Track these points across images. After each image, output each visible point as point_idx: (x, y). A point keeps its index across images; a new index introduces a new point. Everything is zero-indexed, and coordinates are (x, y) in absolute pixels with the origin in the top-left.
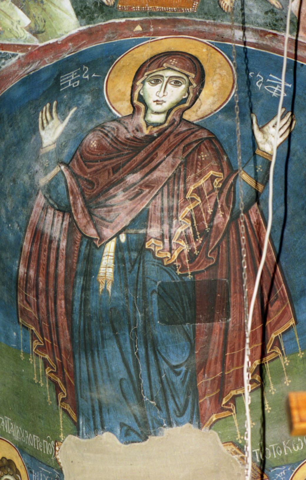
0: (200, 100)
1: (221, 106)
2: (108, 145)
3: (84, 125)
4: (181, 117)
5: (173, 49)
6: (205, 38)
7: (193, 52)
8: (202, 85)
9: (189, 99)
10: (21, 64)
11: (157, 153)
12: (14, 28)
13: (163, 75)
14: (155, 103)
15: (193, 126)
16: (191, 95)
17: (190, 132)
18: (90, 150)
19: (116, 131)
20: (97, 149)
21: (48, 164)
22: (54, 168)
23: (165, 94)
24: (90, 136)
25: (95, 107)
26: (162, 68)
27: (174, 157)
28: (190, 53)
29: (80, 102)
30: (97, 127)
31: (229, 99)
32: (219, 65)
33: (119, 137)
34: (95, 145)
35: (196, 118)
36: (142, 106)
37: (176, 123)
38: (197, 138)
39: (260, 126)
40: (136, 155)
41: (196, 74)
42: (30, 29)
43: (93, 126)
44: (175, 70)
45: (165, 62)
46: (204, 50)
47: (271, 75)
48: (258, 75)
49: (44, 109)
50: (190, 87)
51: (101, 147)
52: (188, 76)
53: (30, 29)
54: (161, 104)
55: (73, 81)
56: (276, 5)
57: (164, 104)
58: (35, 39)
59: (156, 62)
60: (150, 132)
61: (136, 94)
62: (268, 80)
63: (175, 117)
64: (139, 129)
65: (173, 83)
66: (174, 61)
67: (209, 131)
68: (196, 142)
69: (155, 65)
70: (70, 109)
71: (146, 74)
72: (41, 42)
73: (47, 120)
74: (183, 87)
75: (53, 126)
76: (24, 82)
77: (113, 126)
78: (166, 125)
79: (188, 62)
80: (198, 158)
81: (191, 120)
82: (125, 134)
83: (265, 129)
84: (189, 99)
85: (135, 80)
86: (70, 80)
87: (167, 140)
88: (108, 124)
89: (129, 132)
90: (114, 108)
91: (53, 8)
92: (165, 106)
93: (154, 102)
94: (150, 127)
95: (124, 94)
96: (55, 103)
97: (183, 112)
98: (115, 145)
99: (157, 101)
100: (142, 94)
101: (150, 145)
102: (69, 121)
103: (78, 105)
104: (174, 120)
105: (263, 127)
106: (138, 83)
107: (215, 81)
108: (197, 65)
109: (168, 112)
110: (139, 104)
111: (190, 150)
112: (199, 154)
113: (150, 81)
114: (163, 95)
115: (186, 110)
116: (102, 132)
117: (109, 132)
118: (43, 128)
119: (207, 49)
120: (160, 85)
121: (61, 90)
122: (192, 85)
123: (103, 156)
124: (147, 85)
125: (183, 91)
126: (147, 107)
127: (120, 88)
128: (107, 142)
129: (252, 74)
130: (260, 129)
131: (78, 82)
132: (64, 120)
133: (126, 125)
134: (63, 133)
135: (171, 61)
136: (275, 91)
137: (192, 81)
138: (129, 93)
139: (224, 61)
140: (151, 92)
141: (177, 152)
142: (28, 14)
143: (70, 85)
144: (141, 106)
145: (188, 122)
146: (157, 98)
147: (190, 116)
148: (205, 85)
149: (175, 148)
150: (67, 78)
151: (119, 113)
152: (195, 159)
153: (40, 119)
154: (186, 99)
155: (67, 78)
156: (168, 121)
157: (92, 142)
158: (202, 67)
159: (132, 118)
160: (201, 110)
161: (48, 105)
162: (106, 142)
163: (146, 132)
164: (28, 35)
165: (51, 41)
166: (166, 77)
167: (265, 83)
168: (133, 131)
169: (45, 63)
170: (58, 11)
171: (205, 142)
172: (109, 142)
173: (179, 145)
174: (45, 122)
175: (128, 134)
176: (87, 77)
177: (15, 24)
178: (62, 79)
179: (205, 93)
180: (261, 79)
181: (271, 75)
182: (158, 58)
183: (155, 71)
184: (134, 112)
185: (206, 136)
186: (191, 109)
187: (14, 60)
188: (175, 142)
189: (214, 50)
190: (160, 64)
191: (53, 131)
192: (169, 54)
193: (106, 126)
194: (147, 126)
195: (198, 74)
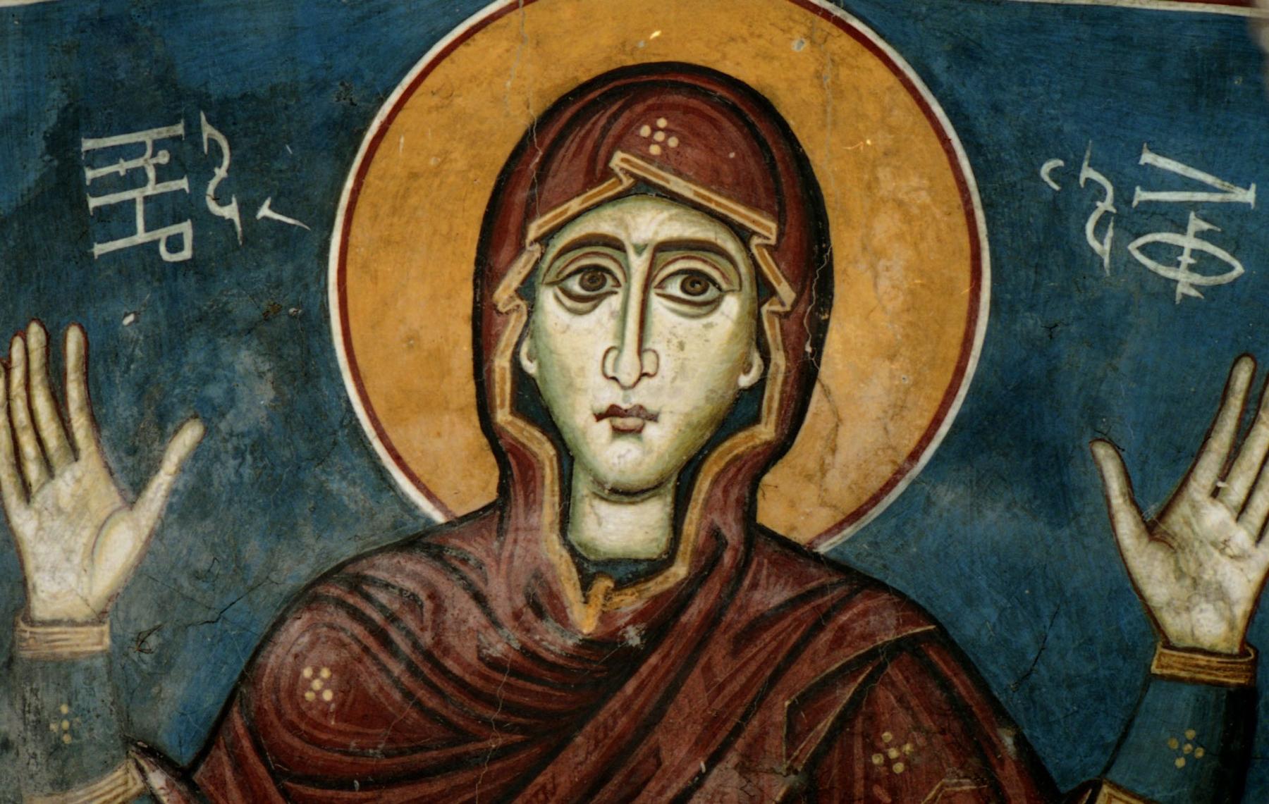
0: (827, 392)
1: (937, 421)
2: (397, 696)
3: (254, 551)
9: (774, 393)
11: (656, 753)
13: (622, 236)
14: (605, 423)
15: (819, 576)
16: (779, 359)
18: (302, 715)
19: (427, 615)
20: (339, 714)
21: (71, 731)
22: (108, 767)
23: (649, 359)
24: (295, 632)
25: (304, 448)
26: (606, 190)
27: (744, 769)
28: (728, 68)
29: (215, 391)
30: (324, 578)
33: (447, 651)
34: (328, 696)
36: (545, 451)
37: (727, 558)
38: (846, 655)
39: (1152, 510)
40: (550, 755)
41: (780, 218)
44: (674, 198)
45: (618, 144)
46: (798, 46)
47: (1147, 158)
48: (1088, 173)
50: (766, 308)
51: (357, 707)
52: (742, 234)
54: (637, 432)
57: (651, 430)
59: (571, 144)
60: (605, 617)
61: (501, 363)
62: (1141, 195)
63: (716, 518)
64: (543, 600)
65: (674, 288)
66: (659, 134)
67: (904, 602)
68: (847, 672)
69: (567, 167)
70: (164, 425)
71: (534, 231)
73: (40, 441)
74: (732, 306)
75: (82, 506)
77: (410, 585)
78: (680, 570)
80: (869, 766)
81: (801, 536)
82: (478, 637)
84: (774, 393)
85: (485, 275)
87: (697, 671)
88: (382, 568)
89: (495, 623)
90: (398, 459)
92: (659, 445)
93: (599, 417)
94: (603, 584)
96: (73, 339)
97: (754, 484)
98: (433, 703)
99: (613, 412)
100: (531, 368)
101: (614, 704)
102: (170, 508)
103: (209, 414)
104: (715, 534)
105: (1164, 513)
106: (504, 294)
107: (879, 254)
109: (681, 481)
110: (523, 427)
111: (824, 726)
112: (872, 747)
113: (559, 282)
114: (639, 363)
115: (765, 469)
116: (355, 614)
117: (393, 618)
118: (26, 491)
119: (809, 37)
120: (614, 302)
121: (99, 249)
122: (773, 292)
123: (376, 757)
125: (734, 336)
126: (567, 457)
128: (387, 682)
129: (1054, 173)
130: (1153, 529)
131: (186, 228)
132: (136, 486)
133: (473, 576)
134: (143, 573)
135: (645, 131)
136: (1186, 259)
140: (577, 344)
141: (761, 737)
143: (141, 237)
144: (534, 447)
145: (791, 553)
146: (609, 396)
147: (792, 504)
148: (839, 289)
149: (746, 717)
150: (122, 167)
151: (430, 496)
152: (859, 770)
154: (758, 388)
155: (122, 167)
156: (686, 548)
157: (307, 673)
158: (801, 162)
159: (501, 532)
160: (840, 458)
162: (386, 679)
163: (586, 620)
166: (639, 250)
167: (1130, 221)
168: (517, 616)
171: (889, 670)
172: (397, 682)
173: (760, 701)
174: (29, 449)
175: (492, 636)
176: (230, 212)
179: (846, 341)
180: (1101, 193)
181: (1147, 158)
182: (578, 119)
183: (575, 205)
184: (503, 489)
185: (891, 636)
186: (789, 457)
188: (741, 679)
189: (846, 42)
190: (593, 159)
191: (86, 535)
193: (374, 582)
194: (586, 584)
195: (792, 216)
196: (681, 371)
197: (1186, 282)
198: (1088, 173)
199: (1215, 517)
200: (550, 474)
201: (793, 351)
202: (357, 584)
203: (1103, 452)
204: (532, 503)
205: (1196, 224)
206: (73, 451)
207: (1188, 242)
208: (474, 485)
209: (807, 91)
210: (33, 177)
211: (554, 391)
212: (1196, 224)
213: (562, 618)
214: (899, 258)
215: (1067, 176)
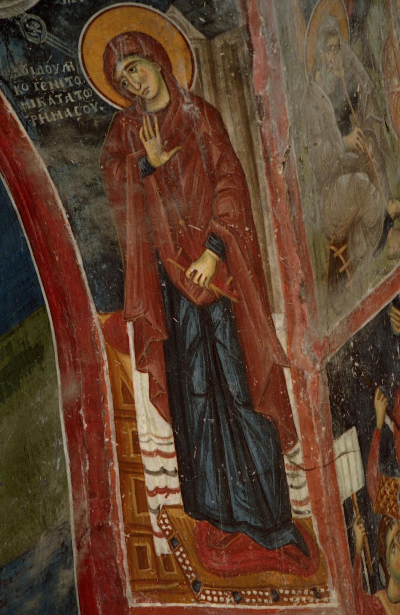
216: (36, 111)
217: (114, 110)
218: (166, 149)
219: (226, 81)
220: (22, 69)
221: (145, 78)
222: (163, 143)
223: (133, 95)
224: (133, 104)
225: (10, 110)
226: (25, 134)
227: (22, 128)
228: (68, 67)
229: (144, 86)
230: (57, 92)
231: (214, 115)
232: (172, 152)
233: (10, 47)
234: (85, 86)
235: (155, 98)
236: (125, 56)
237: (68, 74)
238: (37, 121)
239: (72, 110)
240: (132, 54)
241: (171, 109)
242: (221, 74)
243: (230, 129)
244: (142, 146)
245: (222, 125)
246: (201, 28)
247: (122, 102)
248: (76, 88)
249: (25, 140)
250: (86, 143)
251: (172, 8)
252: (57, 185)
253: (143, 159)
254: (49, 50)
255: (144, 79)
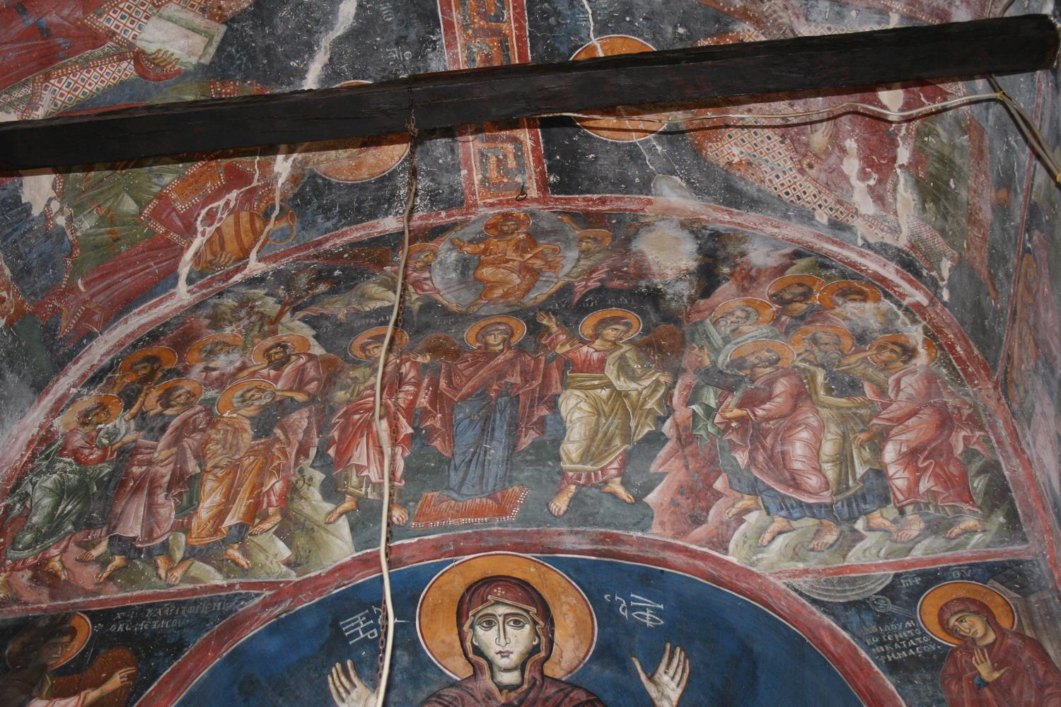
1: (588, 651)
3: (410, 694)
4: (542, 672)
5: (490, 573)
6: (527, 552)
7: (518, 574)
8: (552, 624)
9: (543, 646)
10: (266, 605)
12: (268, 563)
15: (563, 686)
17: (561, 694)
28: (515, 576)
30: (431, 696)
31: (595, 639)
32: (561, 590)
35: (562, 673)
36: (484, 662)
41: (536, 607)
42: (288, 563)
43: (425, 696)
44: (507, 604)
45: (489, 594)
48: (617, 598)
49: (334, 670)
52: (528, 612)
53: (288, 563)
54: (508, 656)
55: (365, 630)
56: (627, 500)
57: (511, 656)
58: (293, 574)
59: (476, 595)
61: (468, 644)
62: (632, 603)
65: (512, 623)
71: (470, 614)
72: (298, 576)
73: (344, 688)
74: (528, 627)
75: (359, 698)
76: (272, 630)
78: (525, 686)
79: (518, 589)
83: (657, 677)
84: (543, 646)
85: (460, 625)
86: (359, 628)
88: (445, 692)
91: (324, 535)
92: (514, 659)
94: (505, 691)
95: (450, 645)
96: (349, 663)
97: (542, 665)
99: (500, 652)
100: (476, 644)
105: (653, 674)
106: (466, 628)
107: (565, 614)
108: (534, 595)
109: (522, 667)
110: (478, 658)
113: (480, 624)
114: (506, 641)
118: (343, 700)
120: (496, 627)
124: (478, 629)
127: (443, 637)
130: (651, 679)
132: (374, 686)
137: (537, 619)
138: (458, 644)
139: (564, 584)
140: (489, 638)
142: (289, 543)
143: (362, 636)
145: (555, 681)
146: (499, 649)
150: (353, 624)
153: (331, 686)
154: (538, 645)
155: (353, 624)
158: (540, 595)
159: (476, 681)
161: (338, 665)
163: (502, 700)
164: (284, 568)
165: (312, 574)
167: (632, 609)
169: (301, 602)
170: (331, 537)
174: (341, 690)
177: (271, 558)
178: (344, 625)
184: (475, 671)
187: (257, 600)
189: (545, 569)
192: (490, 581)
194: (501, 691)
196: (517, 642)
197: (649, 624)
198: (617, 598)
199: (666, 678)
200: (486, 667)
201: (546, 636)
202: (439, 696)
203: (634, 659)
204: (482, 674)
205: (648, 611)
206: (355, 686)
207: (648, 615)
208: (468, 672)
209: (537, 580)
210: (328, 634)
211: (484, 648)
212: (648, 611)
213: (495, 699)
214: (570, 616)
215: (612, 598)
216: (885, 653)
217: (949, 647)
218: (996, 669)
219: (1043, 622)
220: (874, 629)
221: (974, 626)
222: (993, 664)
223: (965, 637)
224: (966, 642)
225: (863, 654)
226: (876, 669)
227: (874, 665)
228: (908, 624)
229: (972, 631)
230: (901, 640)
231: (1037, 646)
232: (1002, 671)
233: (863, 616)
234: (924, 634)
235: (985, 635)
236: (956, 613)
237: (909, 629)
238: (887, 659)
239: (914, 650)
240: (961, 611)
241: (998, 643)
242: (1037, 618)
243: (1051, 653)
244: (976, 669)
245: (1044, 651)
246: (1016, 591)
247: (956, 641)
248: (917, 636)
249: (877, 673)
250: (927, 670)
251: (991, 581)
252: (903, 698)
253: (977, 678)
254: (894, 615)
255: (972, 626)
